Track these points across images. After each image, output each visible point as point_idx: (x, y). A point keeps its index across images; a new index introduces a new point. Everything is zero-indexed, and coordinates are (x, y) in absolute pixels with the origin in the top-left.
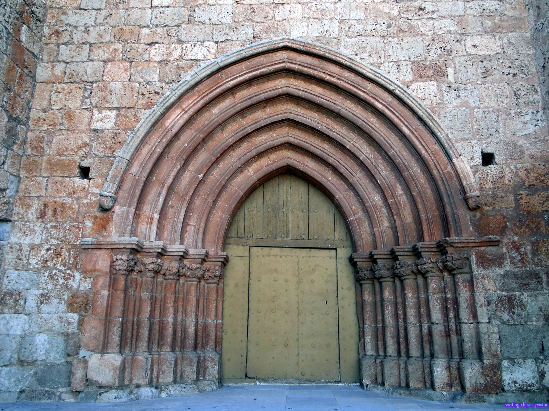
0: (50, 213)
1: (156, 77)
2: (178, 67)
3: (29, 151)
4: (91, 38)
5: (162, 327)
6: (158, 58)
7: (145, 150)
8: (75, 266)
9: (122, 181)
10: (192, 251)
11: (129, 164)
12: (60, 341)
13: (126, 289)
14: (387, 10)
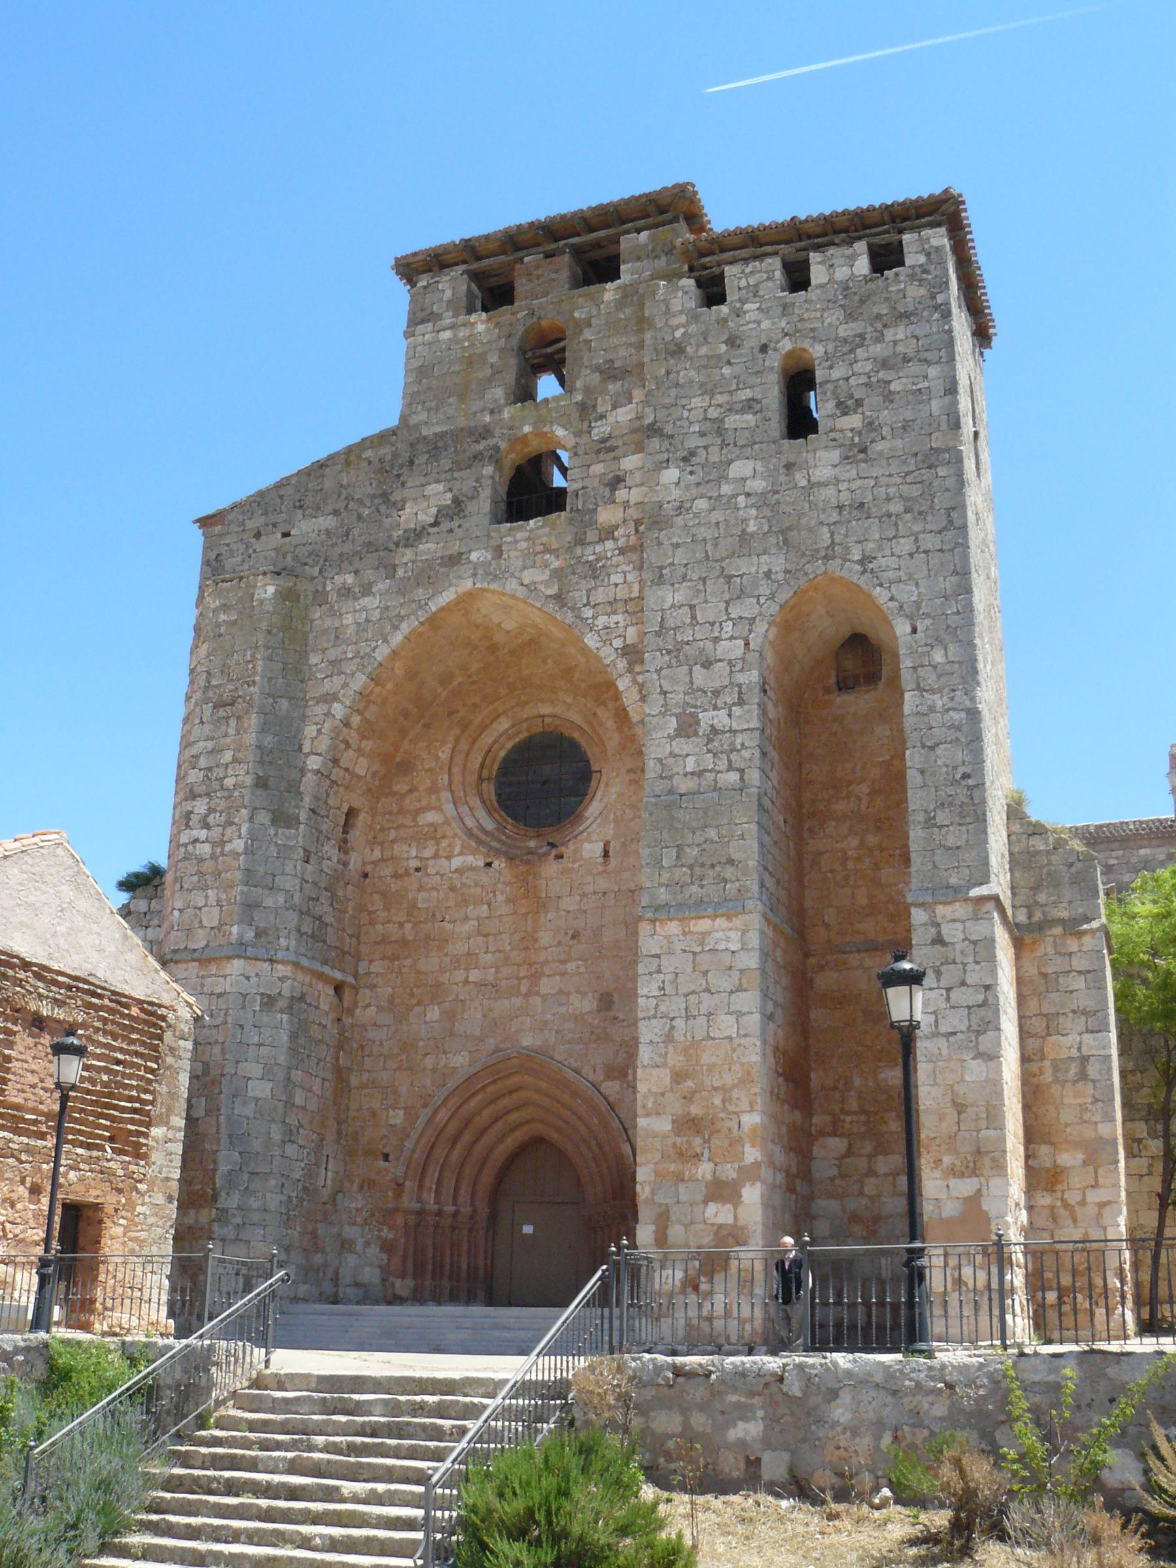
0: (366, 1188)
1: (429, 1081)
2: (444, 1074)
3: (350, 1142)
4: (385, 1051)
5: (442, 1265)
6: (430, 1067)
7: (423, 1141)
8: (383, 1223)
9: (409, 1163)
10: (463, 1210)
11: (413, 1151)
12: (377, 1271)
13: (415, 1239)
14: (590, 1020)
